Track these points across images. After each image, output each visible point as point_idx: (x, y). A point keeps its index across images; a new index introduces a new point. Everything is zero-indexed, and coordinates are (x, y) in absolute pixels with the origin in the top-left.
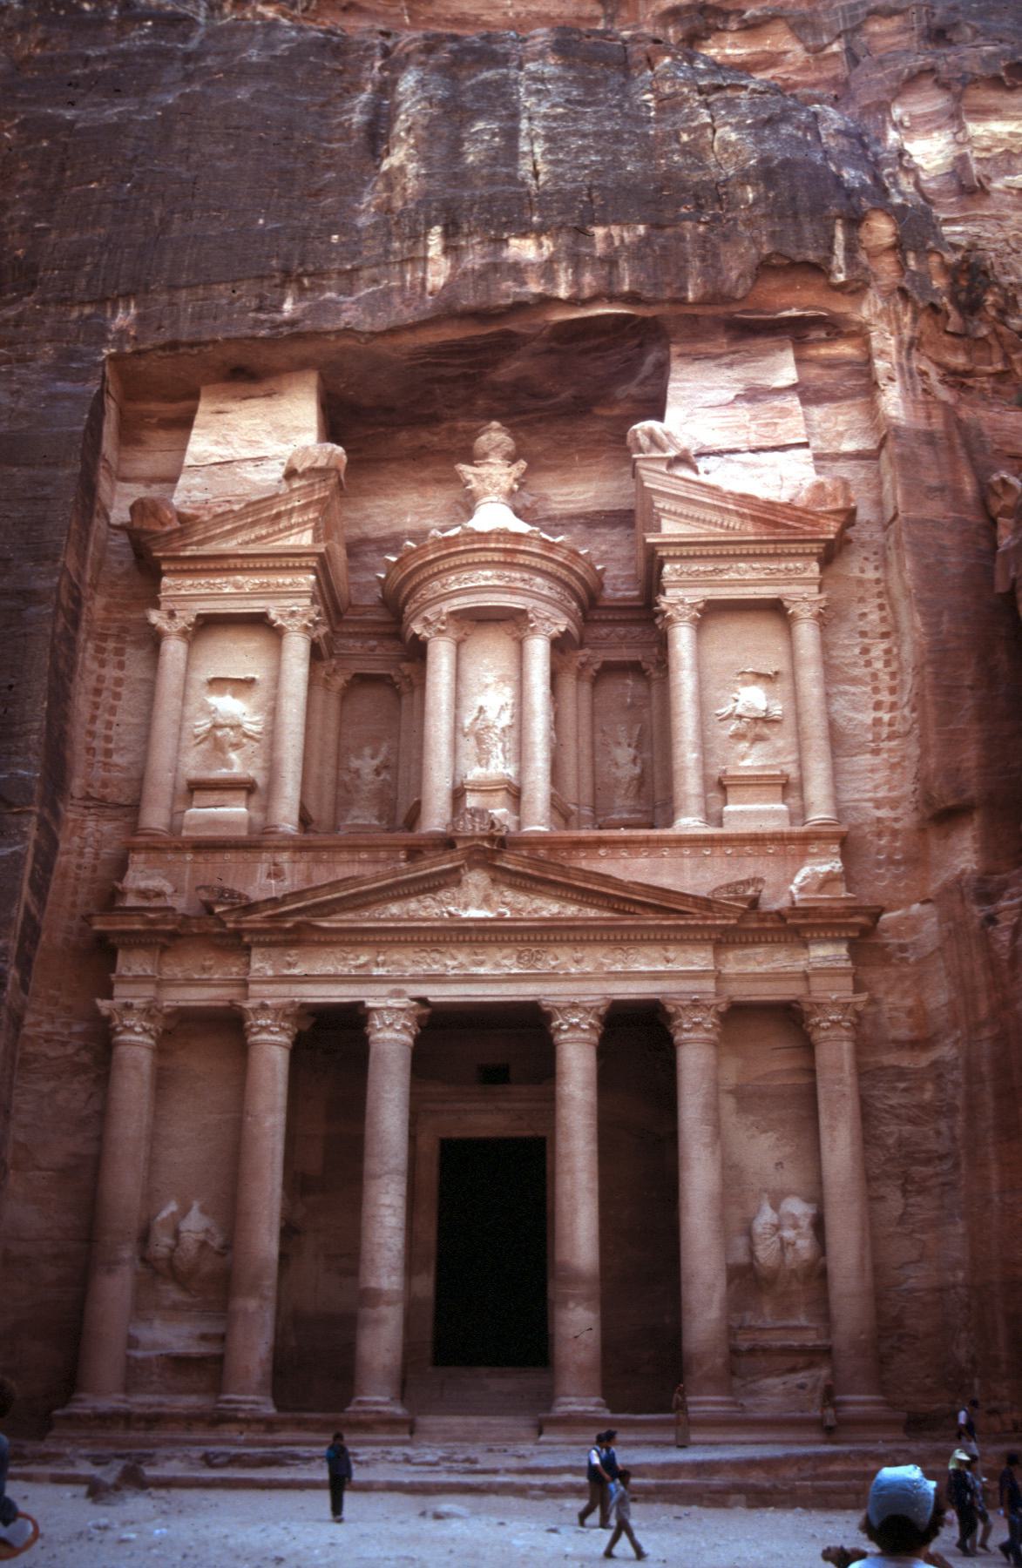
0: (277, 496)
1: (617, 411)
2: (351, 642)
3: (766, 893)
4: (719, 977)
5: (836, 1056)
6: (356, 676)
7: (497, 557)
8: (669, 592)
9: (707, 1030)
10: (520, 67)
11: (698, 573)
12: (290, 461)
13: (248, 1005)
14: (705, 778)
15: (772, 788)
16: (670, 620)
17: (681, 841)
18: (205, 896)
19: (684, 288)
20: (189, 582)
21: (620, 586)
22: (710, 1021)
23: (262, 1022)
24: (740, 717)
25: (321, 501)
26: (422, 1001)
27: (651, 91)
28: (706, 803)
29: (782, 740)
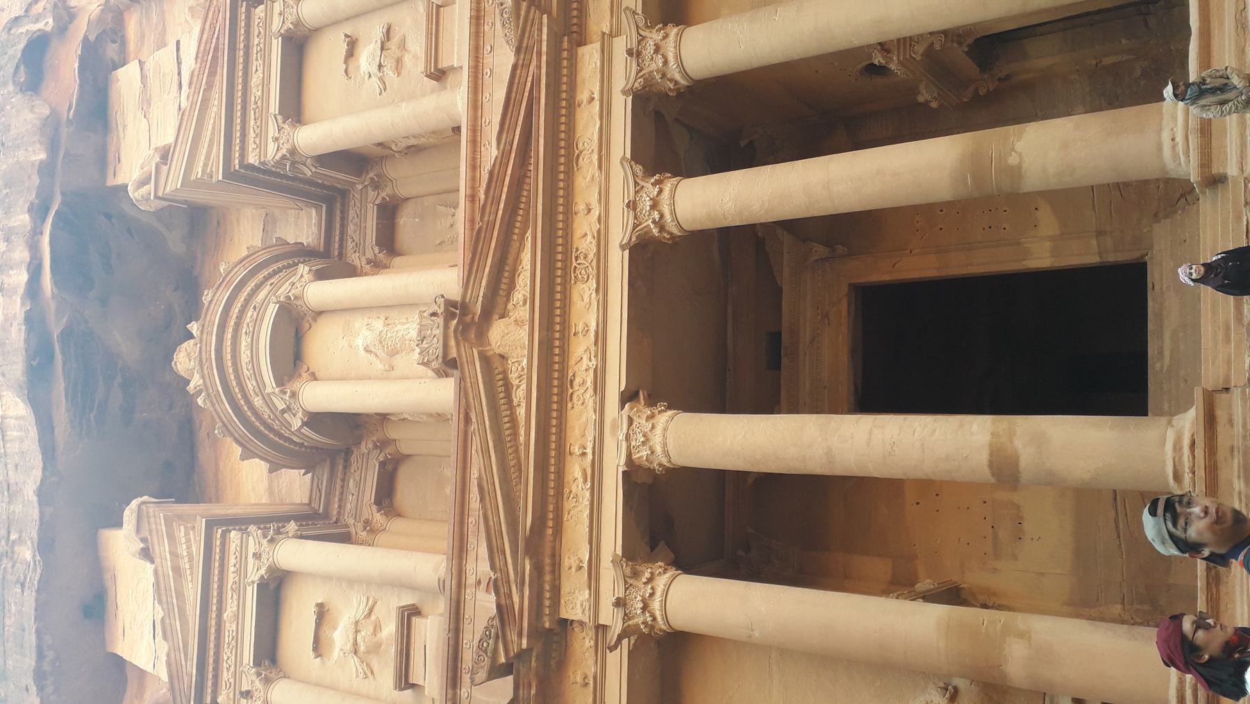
0: (156, 572)
2: (349, 506)
6: (378, 502)
7: (229, 335)
12: (134, 555)
13: (617, 628)
16: (293, 151)
17: (475, 105)
18: (482, 675)
20: (225, 674)
21: (303, 227)
22: (655, 36)
23: (640, 605)
24: (380, 66)
25: (168, 522)
26: (628, 397)
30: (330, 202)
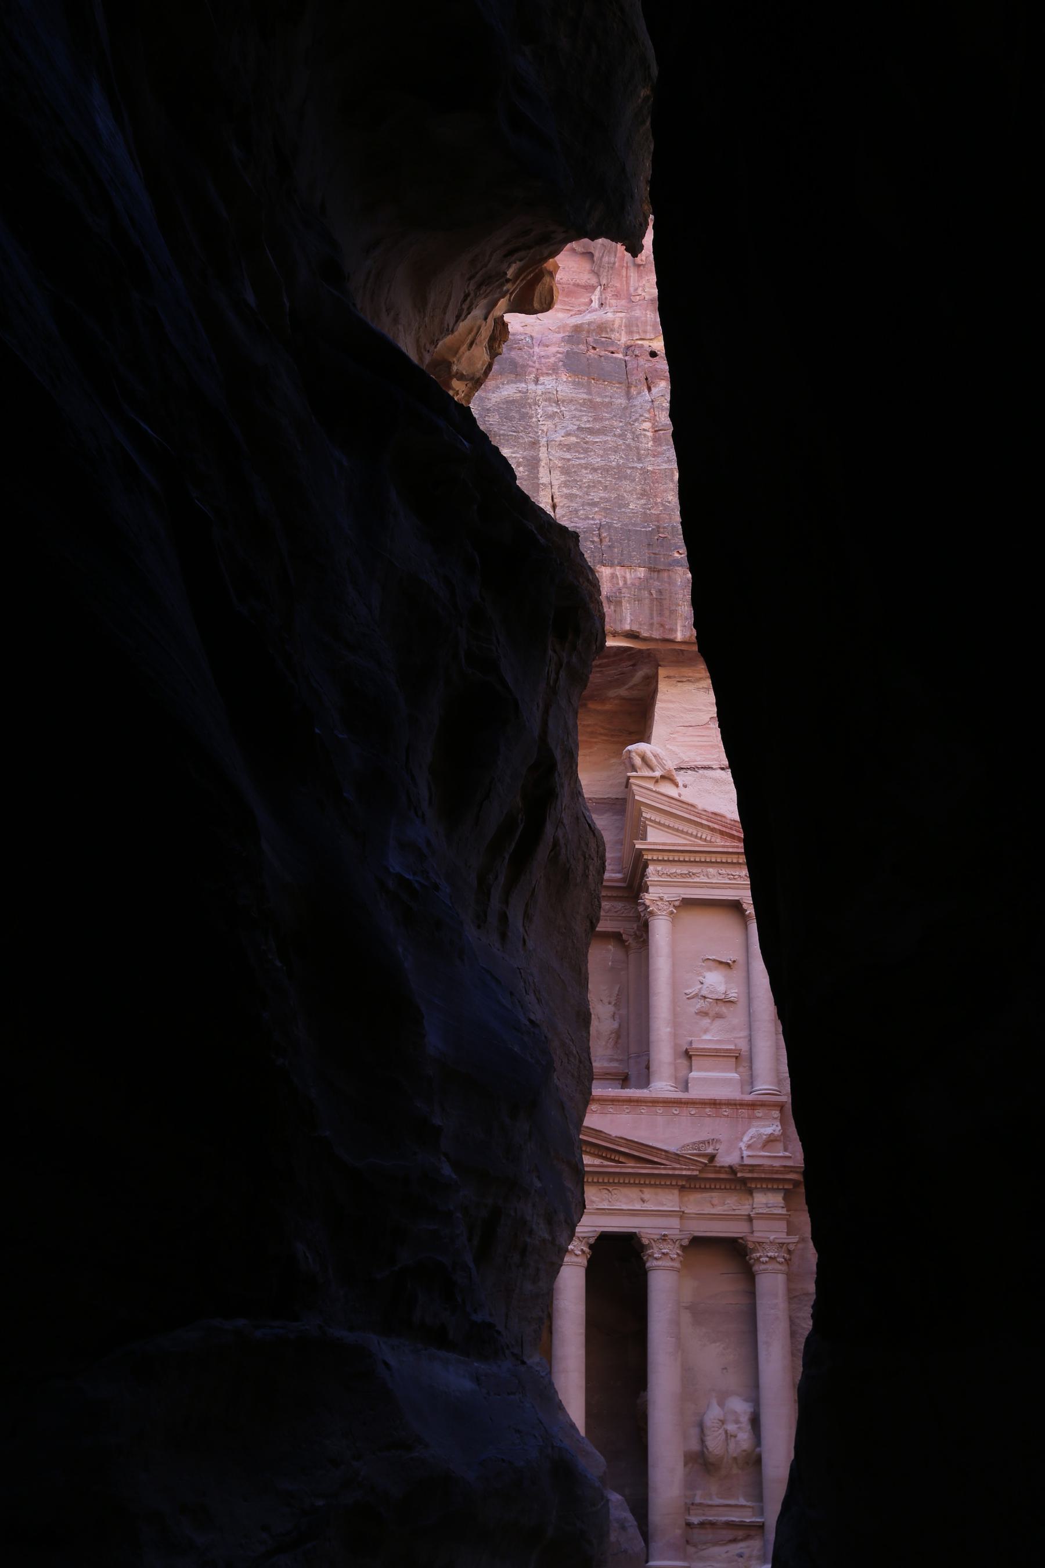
1: (608, 707)
3: (722, 1148)
4: (682, 1215)
5: (772, 1285)
8: (651, 889)
9: (672, 1259)
10: (536, 381)
11: (675, 875)
14: (676, 1046)
15: (729, 1059)
16: (651, 913)
17: (655, 1102)
19: (673, 630)
22: (674, 1251)
24: (705, 997)
27: (649, 420)
28: (676, 1069)
29: (736, 1017)
30: (630, 887)
